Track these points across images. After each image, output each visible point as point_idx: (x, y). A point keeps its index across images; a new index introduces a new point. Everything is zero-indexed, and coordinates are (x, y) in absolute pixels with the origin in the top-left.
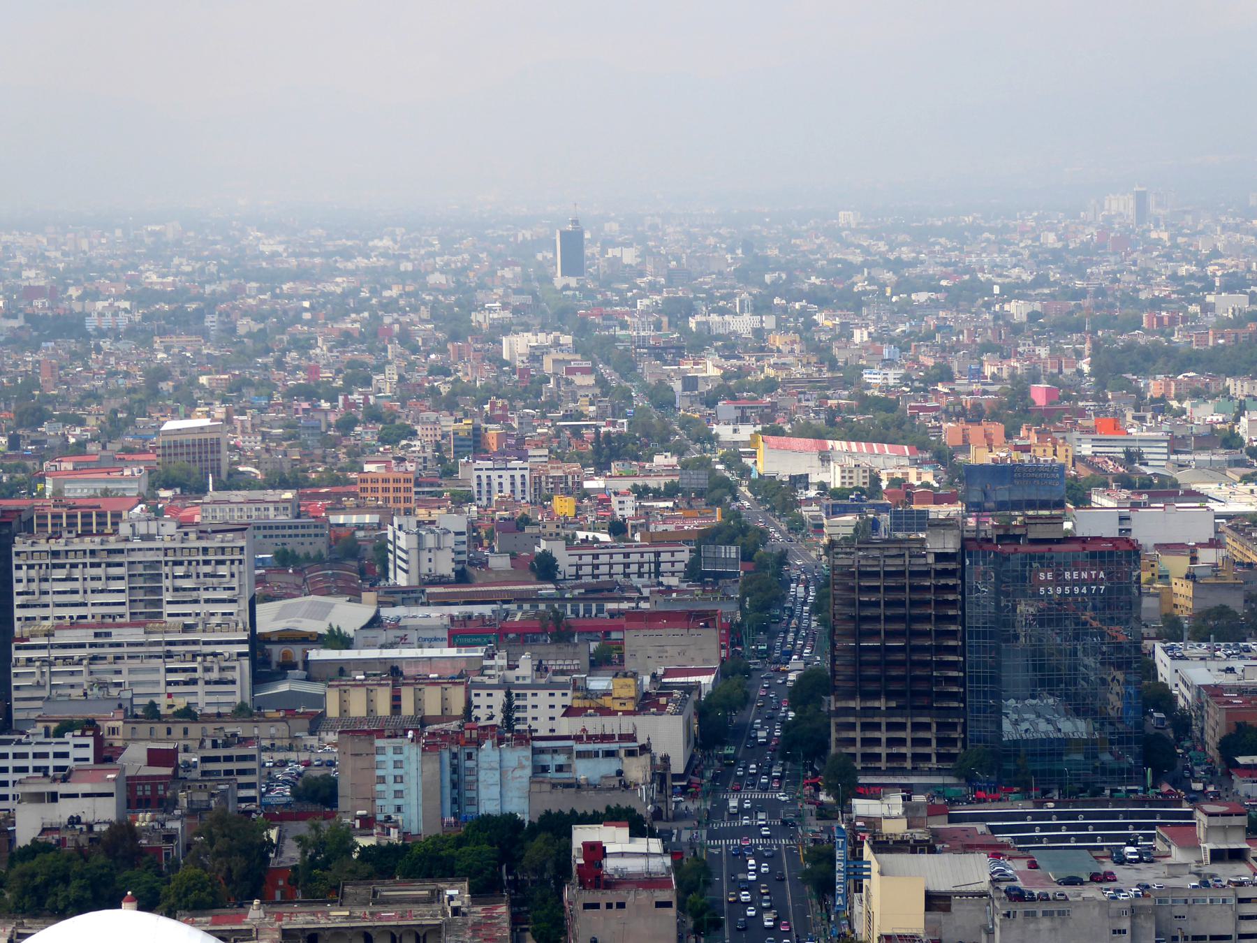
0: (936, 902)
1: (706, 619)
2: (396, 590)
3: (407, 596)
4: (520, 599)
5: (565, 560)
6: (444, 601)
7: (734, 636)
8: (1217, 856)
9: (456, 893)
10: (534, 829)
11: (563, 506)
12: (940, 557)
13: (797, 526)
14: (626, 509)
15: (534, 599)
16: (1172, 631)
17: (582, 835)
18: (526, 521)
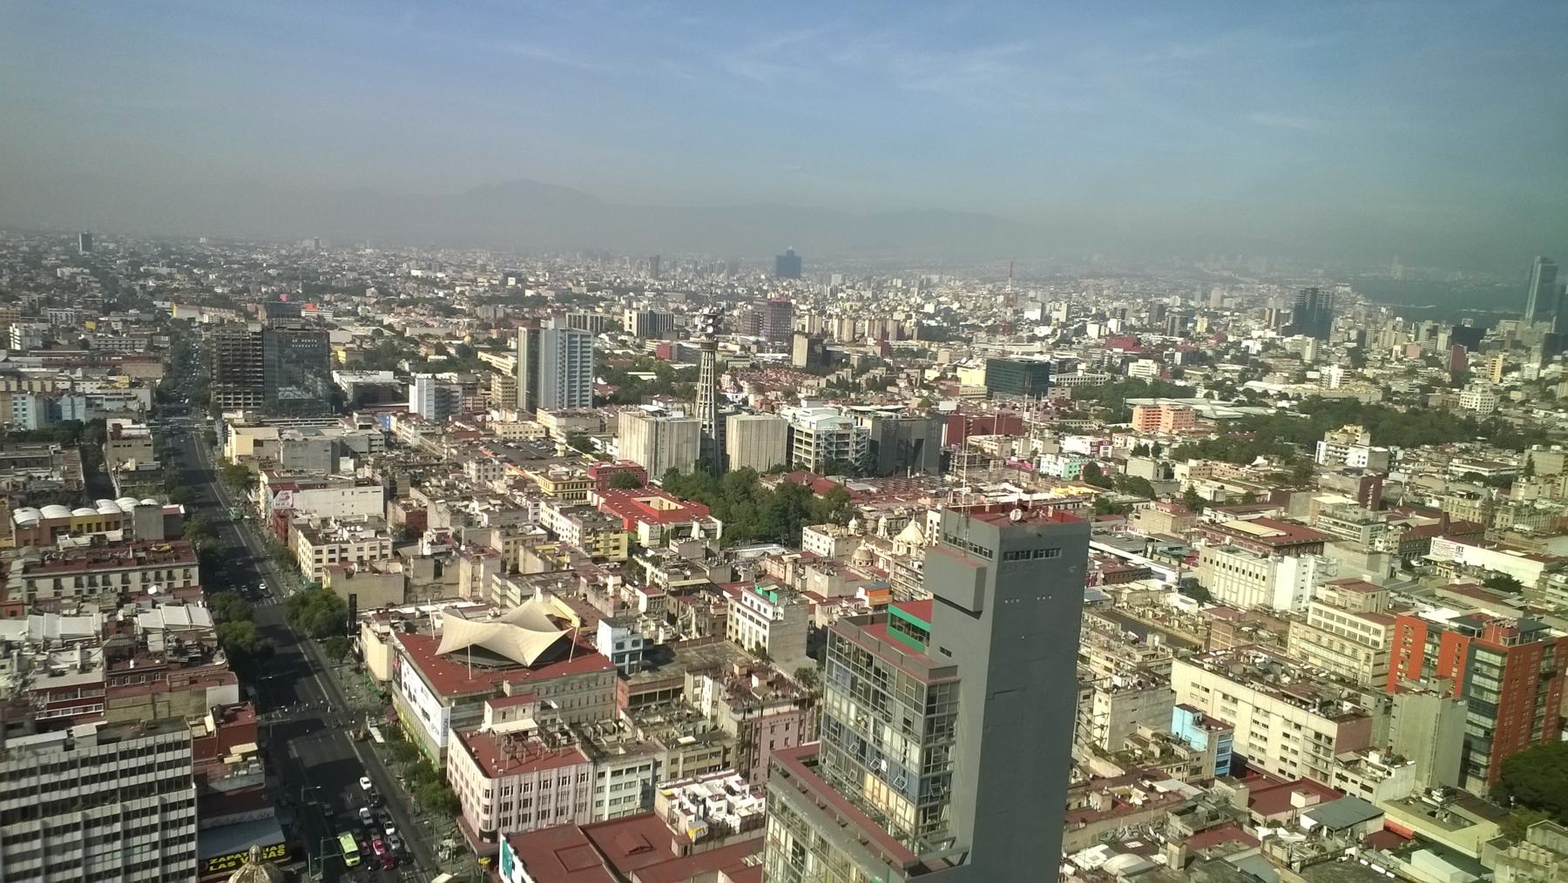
0: (258, 443)
1: (156, 360)
2: (15, 351)
3: (16, 353)
4: (73, 355)
5: (93, 343)
6: (38, 355)
7: (168, 367)
8: (361, 427)
9: (55, 447)
10: (88, 425)
11: (90, 325)
12: (255, 333)
13: (193, 335)
14: (119, 327)
15: (80, 355)
16: (340, 367)
17: (110, 423)
18: (74, 329)
